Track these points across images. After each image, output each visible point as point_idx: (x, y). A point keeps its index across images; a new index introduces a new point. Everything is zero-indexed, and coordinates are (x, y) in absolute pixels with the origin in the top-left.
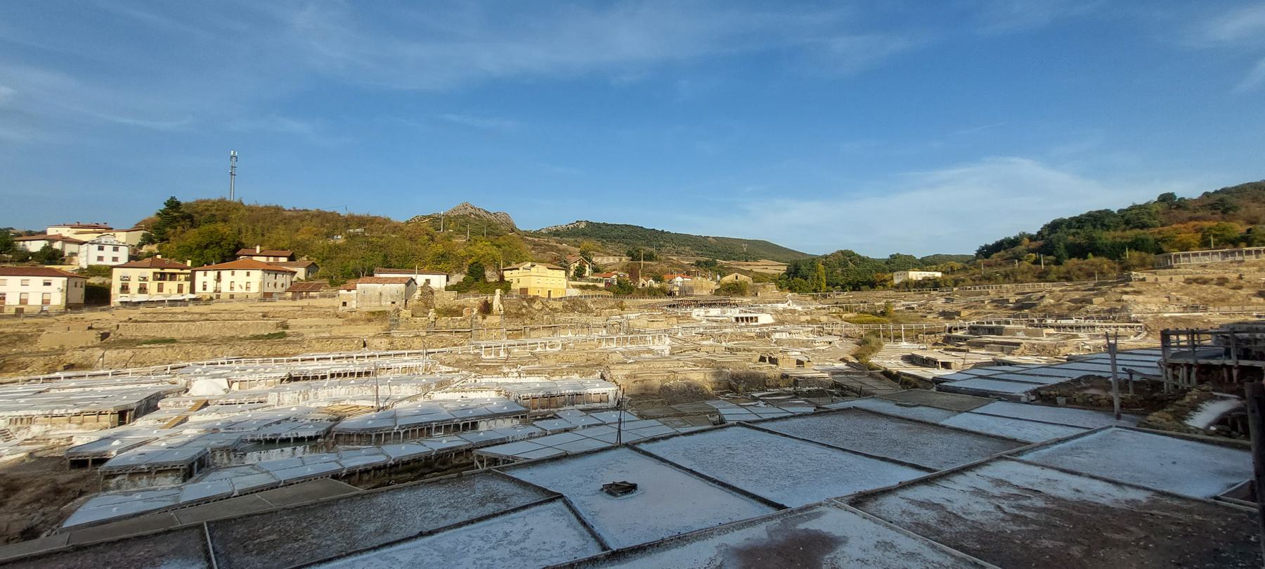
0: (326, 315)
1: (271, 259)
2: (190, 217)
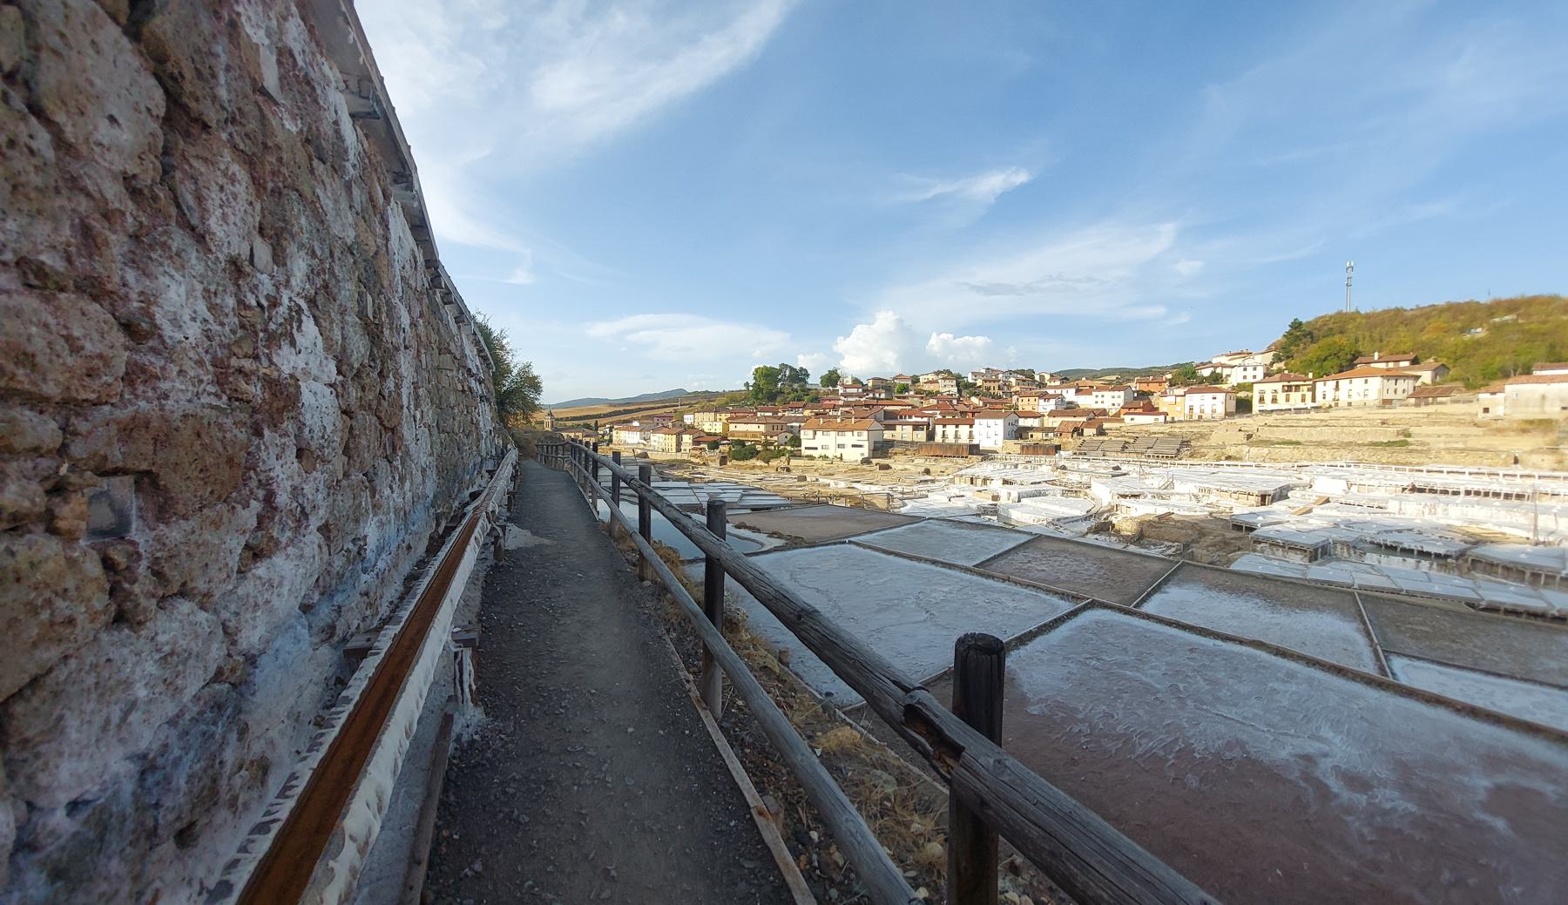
0: (1460, 423)
1: (1391, 365)
2: (1310, 333)
